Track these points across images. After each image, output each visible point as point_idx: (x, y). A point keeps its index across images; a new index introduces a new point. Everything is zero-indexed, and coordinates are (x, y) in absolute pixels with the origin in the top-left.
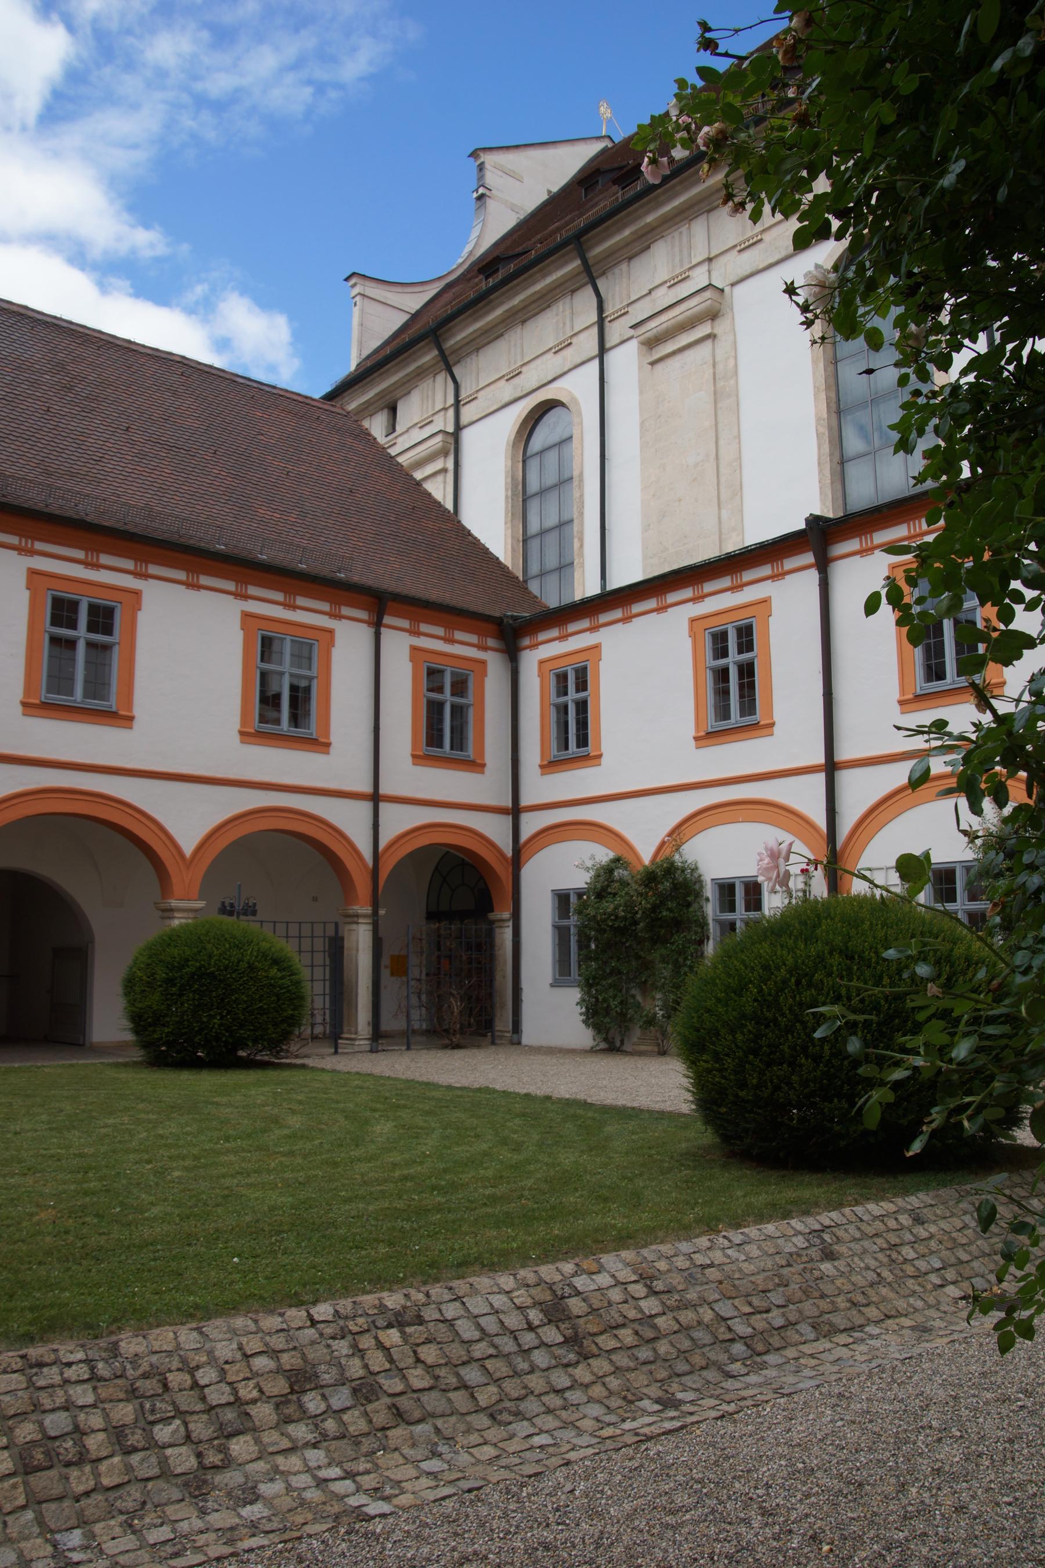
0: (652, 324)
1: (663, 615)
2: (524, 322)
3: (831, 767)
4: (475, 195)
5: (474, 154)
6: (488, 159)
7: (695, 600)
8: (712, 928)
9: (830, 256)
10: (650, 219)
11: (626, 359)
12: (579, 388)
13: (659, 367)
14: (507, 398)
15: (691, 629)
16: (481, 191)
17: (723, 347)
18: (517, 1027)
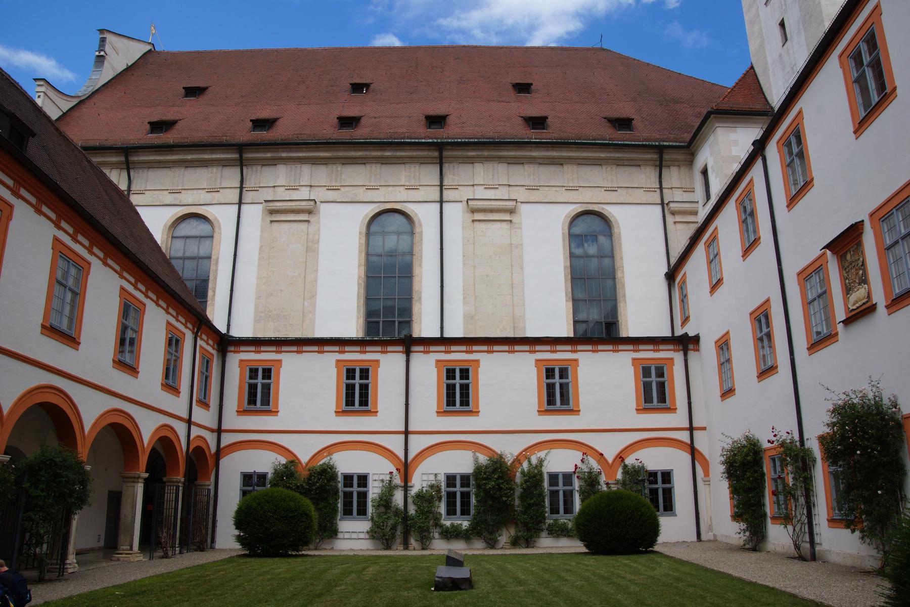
0: (278, 204)
1: (321, 355)
2: (186, 167)
3: (407, 433)
4: (97, 53)
5: (102, 31)
6: (110, 38)
7: (340, 352)
8: (341, 494)
9: (372, 210)
10: (284, 155)
11: (253, 214)
12: (224, 216)
13: (276, 224)
14: (168, 203)
15: (337, 364)
16: (102, 53)
17: (312, 228)
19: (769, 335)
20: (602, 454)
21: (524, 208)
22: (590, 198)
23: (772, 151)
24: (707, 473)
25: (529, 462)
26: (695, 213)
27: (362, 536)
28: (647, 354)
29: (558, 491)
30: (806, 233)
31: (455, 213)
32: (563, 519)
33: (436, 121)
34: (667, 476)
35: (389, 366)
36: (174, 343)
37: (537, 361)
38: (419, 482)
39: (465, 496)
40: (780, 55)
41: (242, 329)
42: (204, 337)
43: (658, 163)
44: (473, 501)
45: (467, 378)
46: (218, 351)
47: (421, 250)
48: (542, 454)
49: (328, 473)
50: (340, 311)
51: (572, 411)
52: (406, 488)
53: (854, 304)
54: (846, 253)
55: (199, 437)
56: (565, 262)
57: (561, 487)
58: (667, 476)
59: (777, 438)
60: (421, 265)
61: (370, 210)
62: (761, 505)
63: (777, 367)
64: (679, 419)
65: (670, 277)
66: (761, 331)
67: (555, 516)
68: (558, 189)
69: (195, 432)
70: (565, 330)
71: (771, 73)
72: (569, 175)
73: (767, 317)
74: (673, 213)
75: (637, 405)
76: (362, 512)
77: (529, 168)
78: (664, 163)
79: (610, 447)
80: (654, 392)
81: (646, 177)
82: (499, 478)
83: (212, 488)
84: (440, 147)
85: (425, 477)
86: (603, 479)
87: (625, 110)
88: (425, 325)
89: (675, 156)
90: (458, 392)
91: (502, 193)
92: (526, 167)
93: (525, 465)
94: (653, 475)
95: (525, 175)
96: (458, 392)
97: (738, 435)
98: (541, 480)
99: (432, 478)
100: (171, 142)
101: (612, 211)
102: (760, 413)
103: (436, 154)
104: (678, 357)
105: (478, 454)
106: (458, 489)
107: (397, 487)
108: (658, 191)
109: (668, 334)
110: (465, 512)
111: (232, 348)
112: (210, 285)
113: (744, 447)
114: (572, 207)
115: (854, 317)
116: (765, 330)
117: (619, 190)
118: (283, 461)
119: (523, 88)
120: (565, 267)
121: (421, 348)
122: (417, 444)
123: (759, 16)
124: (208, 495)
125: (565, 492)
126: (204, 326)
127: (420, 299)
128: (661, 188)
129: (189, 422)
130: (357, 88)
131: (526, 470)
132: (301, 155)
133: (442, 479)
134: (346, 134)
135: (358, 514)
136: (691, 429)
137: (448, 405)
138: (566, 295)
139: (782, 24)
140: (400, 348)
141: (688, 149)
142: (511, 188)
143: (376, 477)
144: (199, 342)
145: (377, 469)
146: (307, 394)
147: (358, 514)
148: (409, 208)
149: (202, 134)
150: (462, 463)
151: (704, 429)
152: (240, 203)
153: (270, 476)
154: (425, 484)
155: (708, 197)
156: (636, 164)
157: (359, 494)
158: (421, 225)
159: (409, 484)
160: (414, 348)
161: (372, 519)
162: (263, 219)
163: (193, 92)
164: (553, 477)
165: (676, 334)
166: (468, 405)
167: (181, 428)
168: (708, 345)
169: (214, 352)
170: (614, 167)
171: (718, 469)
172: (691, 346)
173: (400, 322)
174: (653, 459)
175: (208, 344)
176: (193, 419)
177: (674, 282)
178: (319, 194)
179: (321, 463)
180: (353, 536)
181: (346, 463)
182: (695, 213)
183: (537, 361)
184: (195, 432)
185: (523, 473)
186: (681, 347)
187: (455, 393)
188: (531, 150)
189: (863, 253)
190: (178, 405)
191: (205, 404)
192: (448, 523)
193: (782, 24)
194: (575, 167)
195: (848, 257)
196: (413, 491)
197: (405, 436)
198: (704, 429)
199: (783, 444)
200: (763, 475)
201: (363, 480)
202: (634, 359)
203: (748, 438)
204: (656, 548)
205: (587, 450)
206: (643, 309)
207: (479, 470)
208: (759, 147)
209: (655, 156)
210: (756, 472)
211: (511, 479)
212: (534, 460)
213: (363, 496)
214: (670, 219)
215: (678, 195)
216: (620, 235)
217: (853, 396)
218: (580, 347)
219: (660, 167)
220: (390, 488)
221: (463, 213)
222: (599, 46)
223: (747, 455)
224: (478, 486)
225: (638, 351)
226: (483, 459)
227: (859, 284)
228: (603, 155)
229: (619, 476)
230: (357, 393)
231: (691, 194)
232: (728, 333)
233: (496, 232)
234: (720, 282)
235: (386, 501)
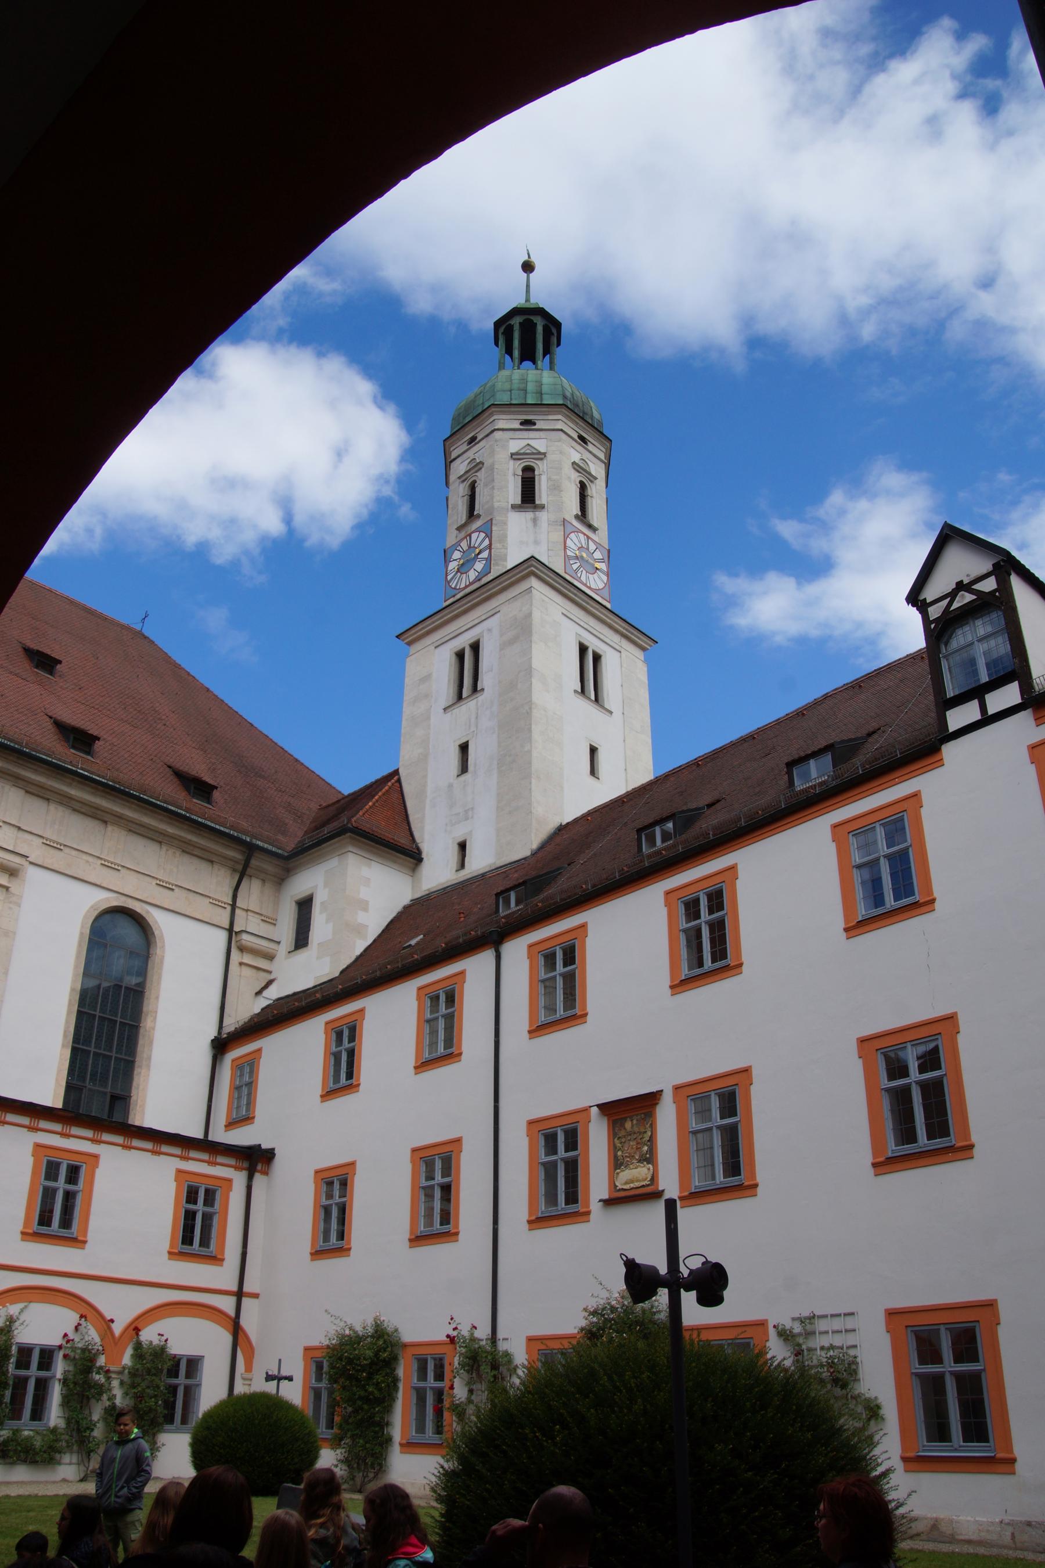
21: (32, 874)
22: (133, 889)
24: (249, 1368)
26: (270, 957)
28: (199, 1166)
29: (26, 1379)
32: (27, 1429)
34: (194, 1364)
37: (37, 1146)
40: (450, 786)
43: (240, 867)
48: (14, 1309)
53: (626, 1183)
54: (625, 1119)
56: (74, 981)
58: (194, 1364)
62: (384, 1424)
64: (224, 1276)
65: (221, 1046)
68: (90, 859)
71: (428, 801)
72: (114, 843)
74: (242, 949)
75: (172, 1246)
77: (56, 812)
78: (249, 871)
80: (195, 1229)
81: (217, 882)
86: (101, 1361)
89: (266, 866)
92: (52, 807)
94: (176, 1360)
95: (72, 828)
97: (359, 1319)
98: (7, 1357)
101: (160, 921)
104: (239, 1179)
108: (229, 908)
109: (198, 1133)
114: (103, 895)
115: (615, 1201)
117: (177, 890)
120: (73, 990)
123: (429, 718)
128: (234, 906)
138: (65, 1036)
139: (464, 748)
141: (290, 861)
142: (21, 834)
151: (256, 1296)
155: (301, 940)
156: (210, 860)
164: (25, 1351)
170: (178, 853)
172: (259, 1167)
174: (182, 1336)
183: (37, 1146)
186: (246, 1164)
188: (70, 785)
189: (653, 1127)
193: (464, 748)
194: (124, 833)
195: (628, 1125)
198: (256, 1296)
200: (396, 1380)
202: (179, 1171)
205: (87, 1311)
206: (171, 1084)
209: (238, 856)
210: (387, 1374)
214: (235, 956)
215: (254, 924)
216: (162, 962)
218: (106, 1137)
219: (242, 873)
222: (138, 627)
225: (188, 1159)
227: (640, 1161)
228: (170, 830)
229: (127, 1359)
231: (271, 927)
232: (353, 1164)
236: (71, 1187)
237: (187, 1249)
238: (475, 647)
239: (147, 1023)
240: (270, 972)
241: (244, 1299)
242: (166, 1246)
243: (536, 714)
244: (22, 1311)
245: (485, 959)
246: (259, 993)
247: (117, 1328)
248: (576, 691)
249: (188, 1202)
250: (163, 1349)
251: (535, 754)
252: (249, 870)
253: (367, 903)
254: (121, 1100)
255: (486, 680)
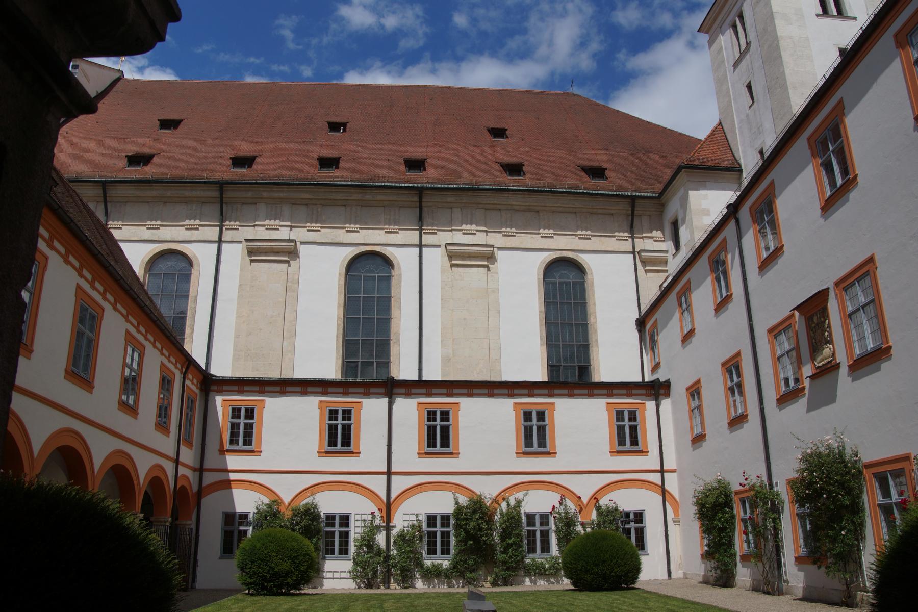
3: (389, 473)
14: (146, 238)
15: (319, 405)
18: (194, 581)
19: (740, 385)
20: (580, 498)
23: (744, 213)
25: (508, 502)
27: (343, 575)
29: (534, 531)
30: (778, 296)
31: (435, 258)
32: (538, 557)
33: (415, 165)
34: (639, 516)
35: (371, 410)
36: (166, 383)
38: (400, 522)
39: (446, 535)
40: (747, 115)
41: (221, 369)
42: (190, 376)
44: (453, 540)
45: (448, 420)
46: (201, 390)
47: (400, 293)
48: (520, 495)
49: (311, 513)
50: (319, 352)
51: (549, 453)
52: (389, 528)
55: (184, 476)
57: (538, 527)
58: (639, 516)
59: (748, 481)
60: (399, 308)
61: (351, 252)
62: (730, 544)
63: (747, 415)
64: (650, 461)
65: (641, 324)
66: (732, 381)
67: (532, 555)
69: (182, 471)
70: (538, 373)
73: (738, 368)
76: (344, 551)
79: (585, 488)
80: (627, 436)
82: (481, 518)
83: (193, 526)
84: (420, 192)
85: (407, 517)
87: (598, 159)
88: (404, 368)
90: (439, 436)
91: (480, 238)
93: (504, 505)
94: (627, 514)
96: (439, 436)
97: (710, 478)
98: (519, 521)
99: (413, 518)
100: (150, 176)
101: (586, 260)
102: (735, 462)
103: (416, 199)
105: (458, 495)
106: (438, 528)
107: (378, 527)
110: (445, 551)
111: (214, 387)
112: (188, 323)
113: (716, 489)
116: (735, 380)
118: (267, 501)
119: (499, 133)
121: (403, 391)
122: (399, 484)
124: (191, 535)
125: (542, 531)
126: (191, 366)
127: (399, 340)
129: (177, 461)
130: (335, 127)
131: (504, 510)
132: (281, 195)
133: (423, 518)
134: (327, 175)
135: (340, 553)
136: (662, 471)
137: (429, 446)
139: (749, 87)
140: (382, 390)
141: (659, 201)
143: (358, 517)
144: (188, 382)
145: (359, 509)
146: (289, 436)
147: (340, 553)
148: (388, 251)
149: (181, 171)
150: (443, 503)
151: (674, 471)
152: (220, 242)
153: (251, 516)
154: (406, 524)
155: (677, 246)
157: (341, 533)
158: (400, 268)
159: (391, 524)
160: (396, 390)
161: (354, 559)
162: (243, 258)
163: (168, 124)
164: (531, 517)
165: (646, 380)
166: (448, 446)
167: (169, 467)
168: (679, 389)
169: (197, 391)
171: (690, 511)
173: (377, 363)
174: (626, 500)
175: (193, 383)
176: (181, 459)
177: (645, 327)
178: (300, 234)
179: (304, 502)
180: (337, 575)
181: (328, 503)
182: (665, 262)
184: (182, 471)
185: (502, 513)
187: (435, 435)
190: (167, 444)
191: (190, 445)
192: (428, 563)
193: (749, 87)
196: (394, 532)
197: (388, 479)
198: (674, 471)
199: (752, 488)
200: (733, 517)
201: (345, 520)
203: (719, 481)
204: (637, 586)
206: (615, 355)
207: (459, 511)
208: (733, 210)
211: (490, 520)
212: (512, 502)
213: (345, 536)
217: (820, 445)
220: (372, 530)
221: (442, 256)
223: (718, 497)
224: (458, 527)
226: (463, 500)
230: (339, 436)
232: (699, 381)
233: (474, 276)
234: (691, 333)
235: (369, 541)
236: (541, 424)
237: (622, 448)
238: (741, 17)
239: (591, 320)
240: (666, 271)
241: (665, 474)
242: (608, 449)
243: (783, 44)
244: (525, 495)
245: (732, 224)
246: (661, 286)
247: (585, 500)
248: (818, 15)
249: (618, 420)
250: (616, 509)
251: (787, 72)
252: (635, 212)
253: (708, 210)
254: (585, 370)
255: (752, 36)
